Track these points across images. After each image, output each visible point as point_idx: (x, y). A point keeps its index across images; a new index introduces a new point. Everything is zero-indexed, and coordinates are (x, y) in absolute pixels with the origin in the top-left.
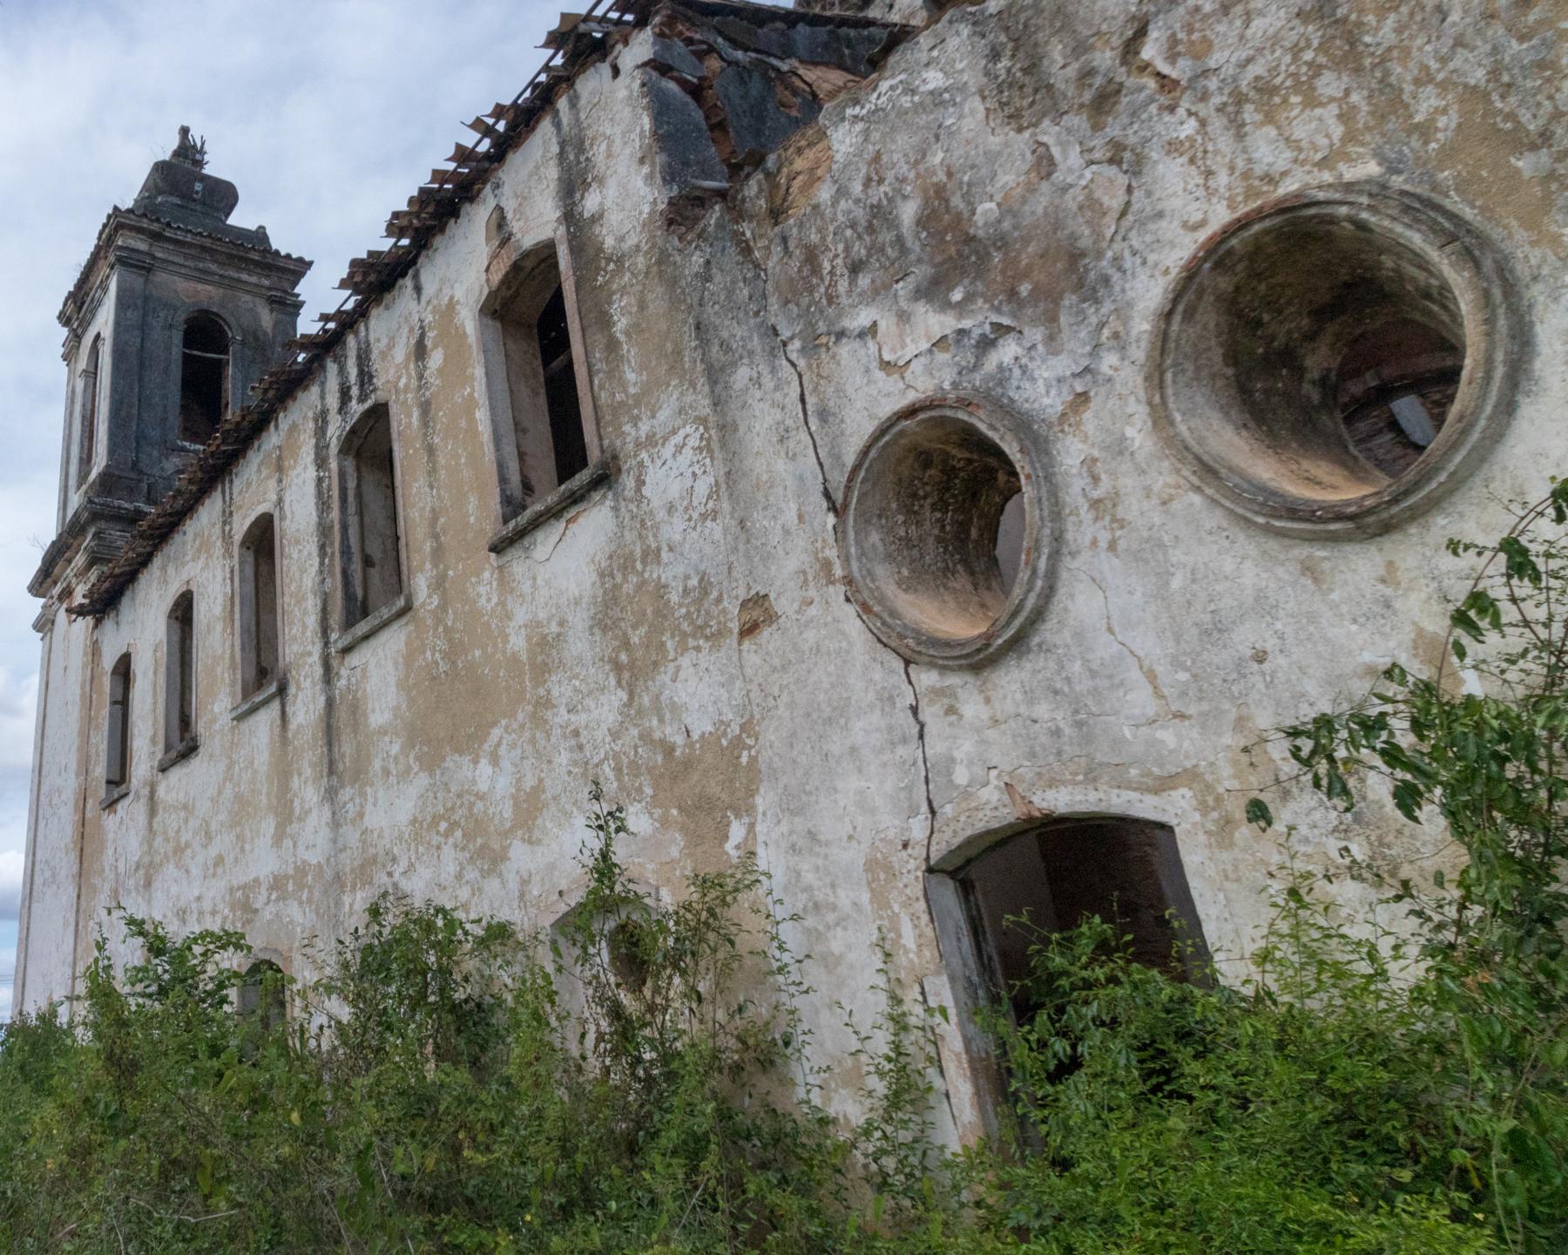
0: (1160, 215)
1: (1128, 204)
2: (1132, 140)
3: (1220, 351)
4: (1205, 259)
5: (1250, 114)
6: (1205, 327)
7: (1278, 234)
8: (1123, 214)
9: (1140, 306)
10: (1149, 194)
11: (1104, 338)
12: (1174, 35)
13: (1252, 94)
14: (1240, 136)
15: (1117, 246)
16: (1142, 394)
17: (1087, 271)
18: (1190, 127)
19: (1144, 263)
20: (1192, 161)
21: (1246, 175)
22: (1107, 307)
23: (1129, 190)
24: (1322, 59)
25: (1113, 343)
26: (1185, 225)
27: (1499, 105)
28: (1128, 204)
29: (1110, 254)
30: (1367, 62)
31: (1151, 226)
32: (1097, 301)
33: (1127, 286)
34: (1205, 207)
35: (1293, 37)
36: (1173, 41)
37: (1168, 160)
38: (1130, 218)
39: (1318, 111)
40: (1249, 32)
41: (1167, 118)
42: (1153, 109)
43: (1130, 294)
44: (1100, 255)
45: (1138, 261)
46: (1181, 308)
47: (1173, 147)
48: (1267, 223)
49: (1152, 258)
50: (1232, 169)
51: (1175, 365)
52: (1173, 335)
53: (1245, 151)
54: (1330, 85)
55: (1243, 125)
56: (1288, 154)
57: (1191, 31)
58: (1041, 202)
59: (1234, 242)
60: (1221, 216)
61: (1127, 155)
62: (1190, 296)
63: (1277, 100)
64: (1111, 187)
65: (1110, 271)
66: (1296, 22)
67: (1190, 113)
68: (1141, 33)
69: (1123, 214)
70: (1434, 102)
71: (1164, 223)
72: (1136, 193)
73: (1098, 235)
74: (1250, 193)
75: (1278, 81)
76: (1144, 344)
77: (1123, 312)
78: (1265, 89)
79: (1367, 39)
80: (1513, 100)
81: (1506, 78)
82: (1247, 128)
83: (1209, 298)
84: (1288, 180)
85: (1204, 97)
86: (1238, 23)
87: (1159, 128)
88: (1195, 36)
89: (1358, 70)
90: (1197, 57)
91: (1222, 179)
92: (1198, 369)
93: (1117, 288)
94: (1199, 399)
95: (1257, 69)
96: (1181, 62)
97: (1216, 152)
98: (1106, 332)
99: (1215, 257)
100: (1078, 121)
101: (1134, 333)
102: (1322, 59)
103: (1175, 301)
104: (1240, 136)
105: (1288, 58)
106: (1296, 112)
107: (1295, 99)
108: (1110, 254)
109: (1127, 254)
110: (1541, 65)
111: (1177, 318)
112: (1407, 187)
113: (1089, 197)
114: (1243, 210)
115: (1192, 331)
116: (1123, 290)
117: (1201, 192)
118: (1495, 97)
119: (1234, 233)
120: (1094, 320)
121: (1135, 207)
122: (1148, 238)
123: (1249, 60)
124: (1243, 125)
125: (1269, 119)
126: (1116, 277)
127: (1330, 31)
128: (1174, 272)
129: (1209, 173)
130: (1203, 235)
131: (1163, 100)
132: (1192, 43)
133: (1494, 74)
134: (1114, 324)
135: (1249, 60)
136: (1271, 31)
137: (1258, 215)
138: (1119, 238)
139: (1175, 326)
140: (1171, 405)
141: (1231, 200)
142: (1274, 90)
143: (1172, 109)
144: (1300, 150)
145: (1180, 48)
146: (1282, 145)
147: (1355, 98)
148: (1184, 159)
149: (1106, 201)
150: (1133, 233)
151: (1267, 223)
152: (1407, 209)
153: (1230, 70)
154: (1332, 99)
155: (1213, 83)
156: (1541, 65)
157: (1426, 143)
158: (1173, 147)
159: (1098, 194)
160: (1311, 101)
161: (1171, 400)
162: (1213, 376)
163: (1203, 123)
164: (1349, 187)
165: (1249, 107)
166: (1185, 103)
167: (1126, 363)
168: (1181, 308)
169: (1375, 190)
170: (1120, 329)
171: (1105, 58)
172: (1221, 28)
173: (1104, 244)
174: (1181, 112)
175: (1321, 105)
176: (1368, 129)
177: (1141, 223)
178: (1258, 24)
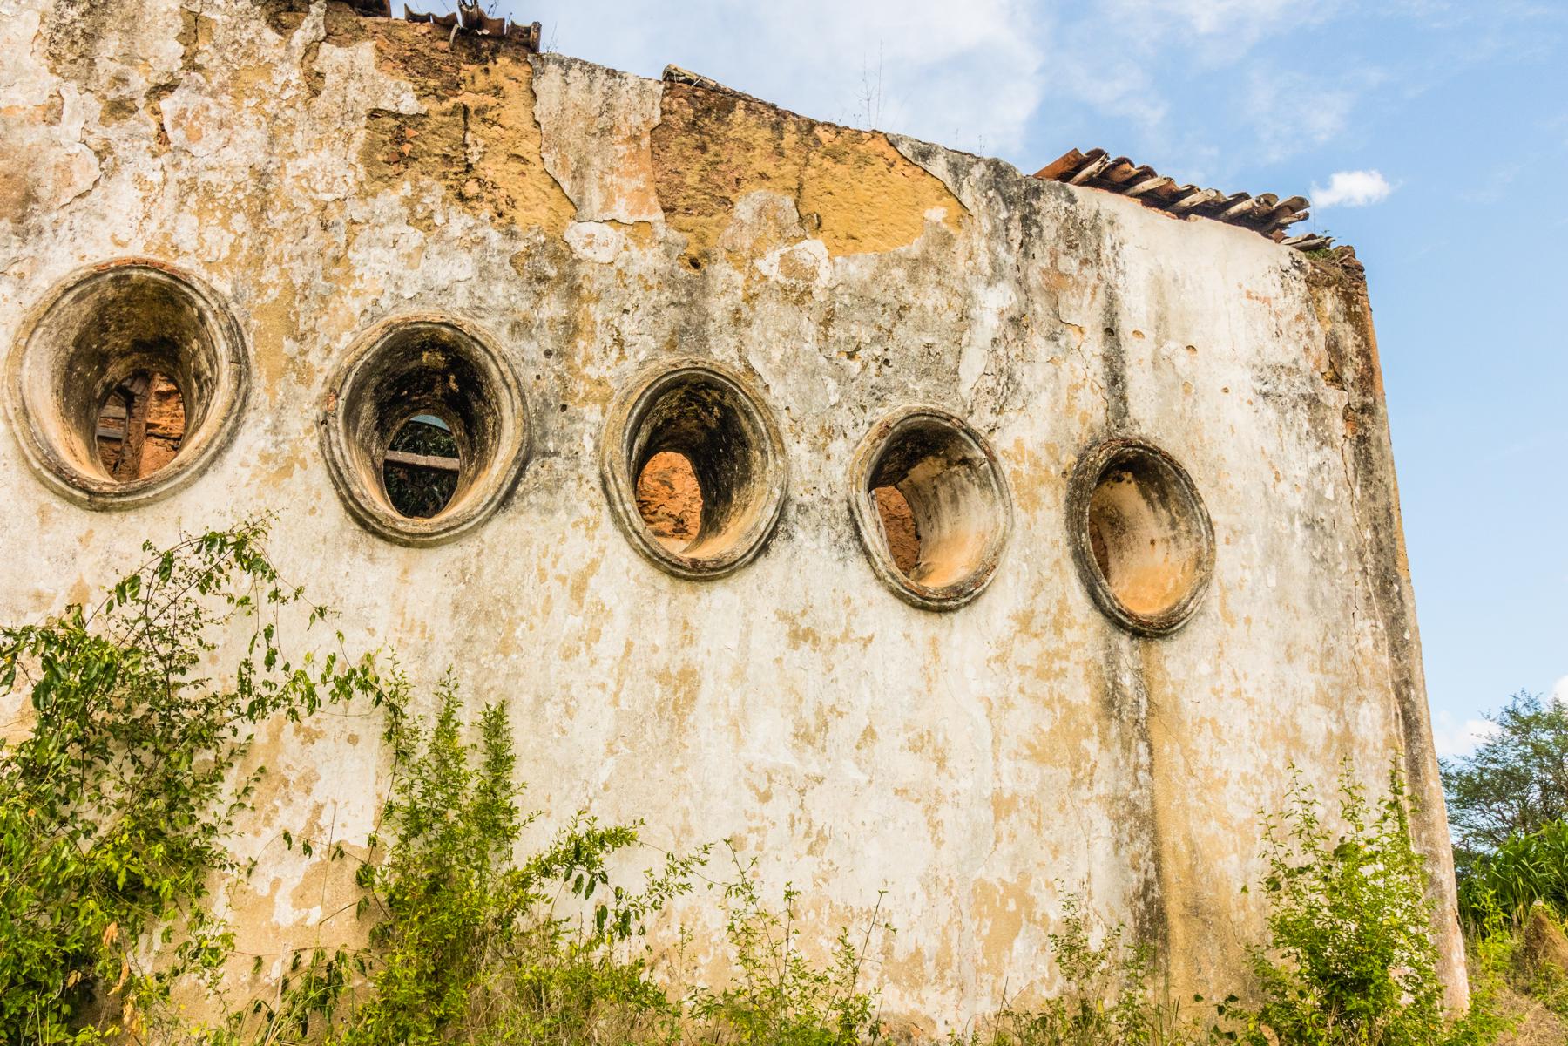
0: (103, 217)
1: (89, 191)
2: (119, 152)
3: (76, 332)
4: (112, 271)
5: (192, 199)
6: (81, 311)
7: (159, 287)
8: (81, 196)
9: (50, 268)
10: (106, 197)
11: (11, 271)
12: (185, 110)
13: (201, 189)
14: (179, 210)
15: (63, 214)
16: (12, 330)
17: (31, 213)
18: (156, 177)
19: (73, 240)
20: (144, 199)
21: (166, 236)
22: (28, 250)
23: (96, 182)
24: (244, 203)
25: (16, 279)
26: (113, 236)
27: (297, 304)
28: (89, 191)
29: (54, 216)
30: (263, 227)
31: (93, 219)
32: (24, 241)
33: (51, 247)
34: (132, 235)
35: (240, 177)
36: (183, 114)
37: (132, 186)
38: (83, 203)
39: (224, 232)
40: (223, 151)
41: (149, 156)
42: (145, 144)
43: (49, 254)
44: (47, 210)
45: (70, 236)
46: (77, 290)
47: (139, 180)
48: (160, 277)
49: (79, 241)
50: (162, 225)
51: (48, 326)
52: (61, 306)
53: (175, 220)
54: (239, 222)
55: (184, 203)
56: (195, 244)
57: (196, 118)
58: (34, 136)
59: (135, 273)
60: (136, 251)
61: (110, 159)
62: (87, 287)
63: (210, 206)
64: (86, 170)
65: (47, 228)
66: (247, 170)
67: (162, 168)
68: (170, 88)
69: (81, 196)
70: (275, 278)
71: (102, 224)
72: (98, 191)
73: (56, 197)
74: (161, 249)
75: (218, 195)
76: (36, 296)
77: (37, 262)
78: (209, 194)
79: (270, 214)
80: (303, 306)
81: (307, 293)
82: (185, 208)
83: (96, 296)
84: (185, 259)
85: (176, 166)
86: (222, 140)
87: (140, 159)
88: (196, 124)
89: (256, 227)
90: (188, 137)
91: (152, 226)
92: (57, 338)
93: (44, 243)
94: (46, 358)
95: (213, 177)
96: (179, 131)
97: (160, 207)
98: (16, 268)
99: (118, 274)
100: (97, 108)
101: (35, 283)
102: (244, 203)
103: (78, 284)
104: (179, 210)
105: (230, 187)
106: (214, 222)
107: (218, 214)
108: (54, 216)
109: (66, 225)
110: (323, 299)
111: (71, 296)
112: (236, 315)
113: (68, 164)
114: (150, 256)
115: (73, 310)
116: (47, 248)
117: (136, 224)
118: (298, 298)
119: (138, 268)
120: (14, 253)
121: (91, 198)
122: (86, 226)
123: (212, 168)
124: (184, 203)
125: (199, 213)
126: (48, 234)
127: (258, 193)
128: (87, 262)
129: (148, 216)
130: (121, 254)
131: (154, 144)
132: (192, 126)
133: (305, 285)
134: (24, 267)
135: (212, 168)
136: (232, 163)
137: (159, 268)
138: (68, 209)
139: (66, 300)
140: (28, 352)
141: (149, 243)
142: (212, 199)
143: (155, 156)
144: (202, 247)
145: (184, 122)
146: (196, 235)
147: (245, 242)
148: (141, 195)
149: (76, 177)
150: (79, 215)
151: (160, 277)
152: (230, 328)
153: (199, 163)
154: (235, 232)
155: (186, 163)
156: (323, 299)
157: (258, 297)
158: (139, 180)
159: (75, 167)
160: (225, 223)
161: (31, 348)
162: (62, 347)
163: (165, 182)
164: (213, 291)
165: (193, 196)
166: (165, 159)
167: (16, 300)
168: (77, 290)
169: (223, 304)
170: (27, 273)
171: (139, 83)
172: (213, 133)
173: (56, 206)
174: (158, 162)
175: (228, 229)
176: (240, 265)
177: (88, 212)
178: (229, 152)
